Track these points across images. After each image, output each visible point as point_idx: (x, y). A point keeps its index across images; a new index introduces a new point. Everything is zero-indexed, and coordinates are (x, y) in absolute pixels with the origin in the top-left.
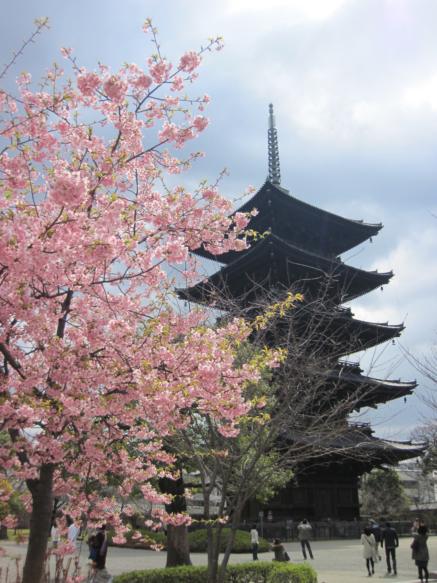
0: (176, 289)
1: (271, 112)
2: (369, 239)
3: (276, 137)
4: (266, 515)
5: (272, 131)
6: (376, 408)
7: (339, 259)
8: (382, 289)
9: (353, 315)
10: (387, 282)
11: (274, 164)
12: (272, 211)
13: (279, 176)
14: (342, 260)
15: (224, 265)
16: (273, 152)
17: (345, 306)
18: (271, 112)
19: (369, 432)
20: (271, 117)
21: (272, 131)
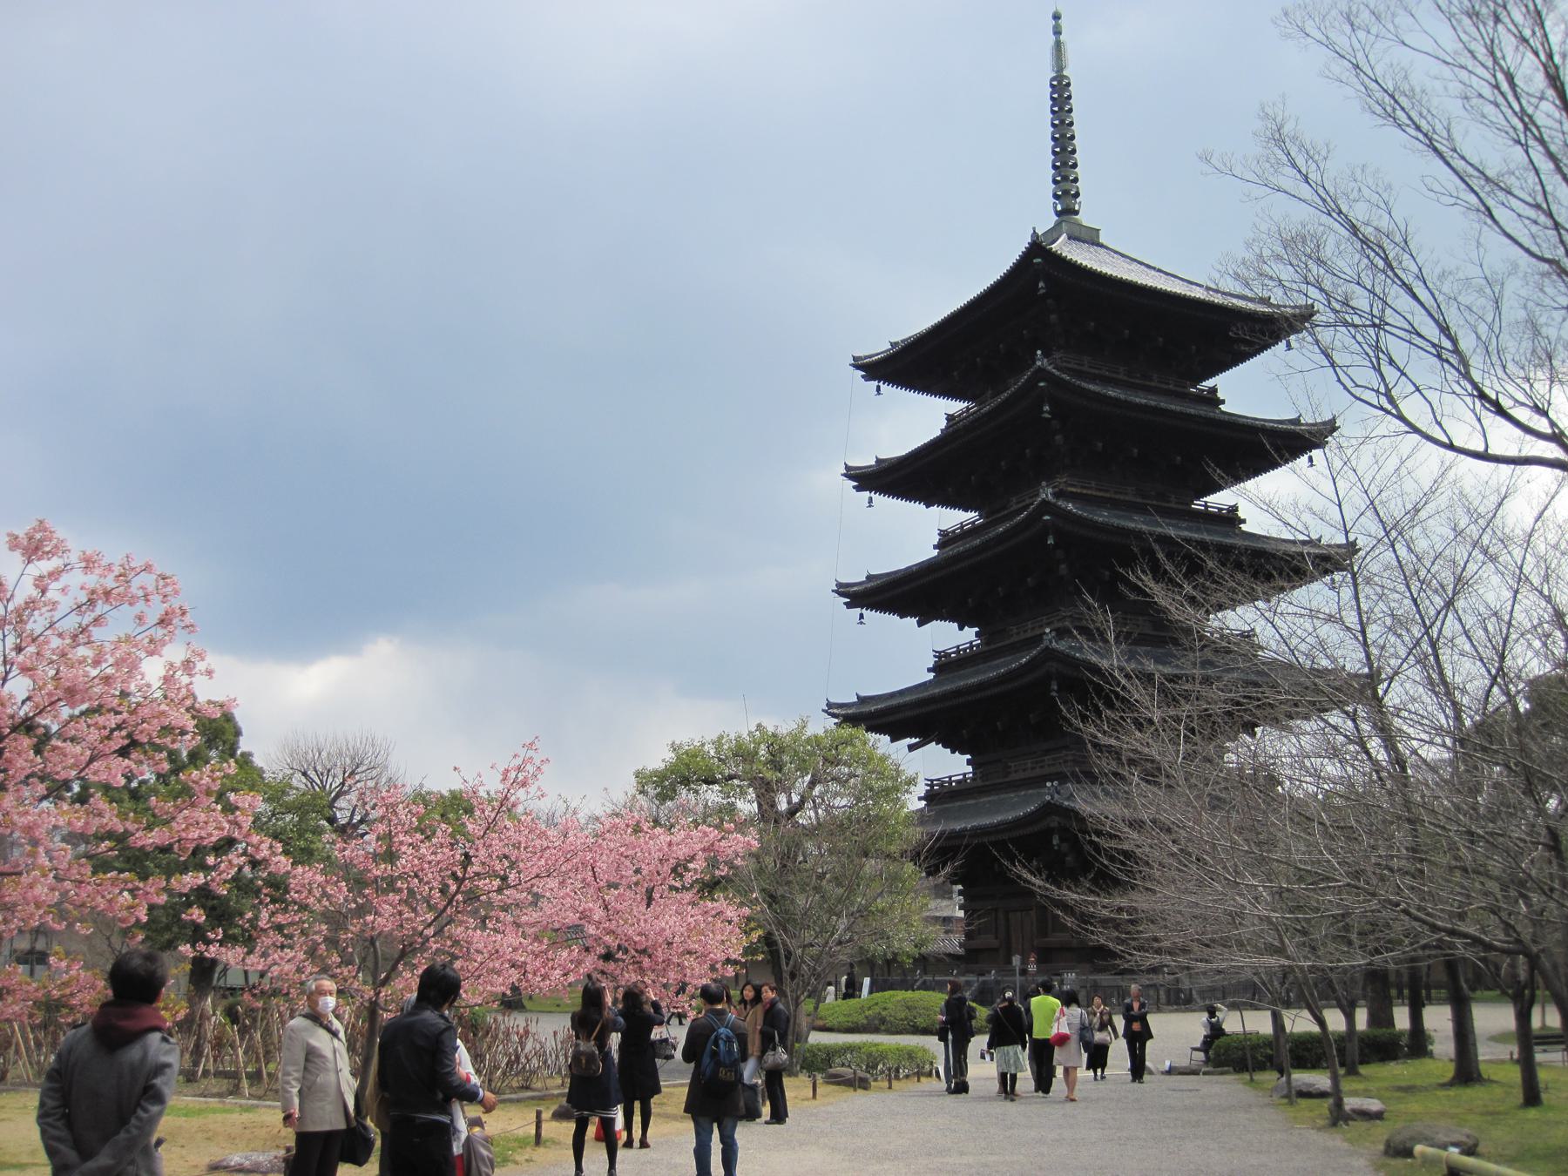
0: (847, 467)
1: (1057, 32)
2: (1282, 345)
3: (1069, 97)
4: (1025, 962)
5: (1060, 83)
6: (1289, 730)
7: (1214, 390)
8: (1311, 459)
9: (1244, 521)
10: (1320, 445)
11: (1065, 164)
12: (1049, 301)
13: (1077, 195)
14: (1220, 395)
15: (956, 406)
16: (1063, 136)
17: (1220, 499)
18: (1057, 32)
19: (1273, 781)
20: (1058, 46)
21: (1060, 83)
